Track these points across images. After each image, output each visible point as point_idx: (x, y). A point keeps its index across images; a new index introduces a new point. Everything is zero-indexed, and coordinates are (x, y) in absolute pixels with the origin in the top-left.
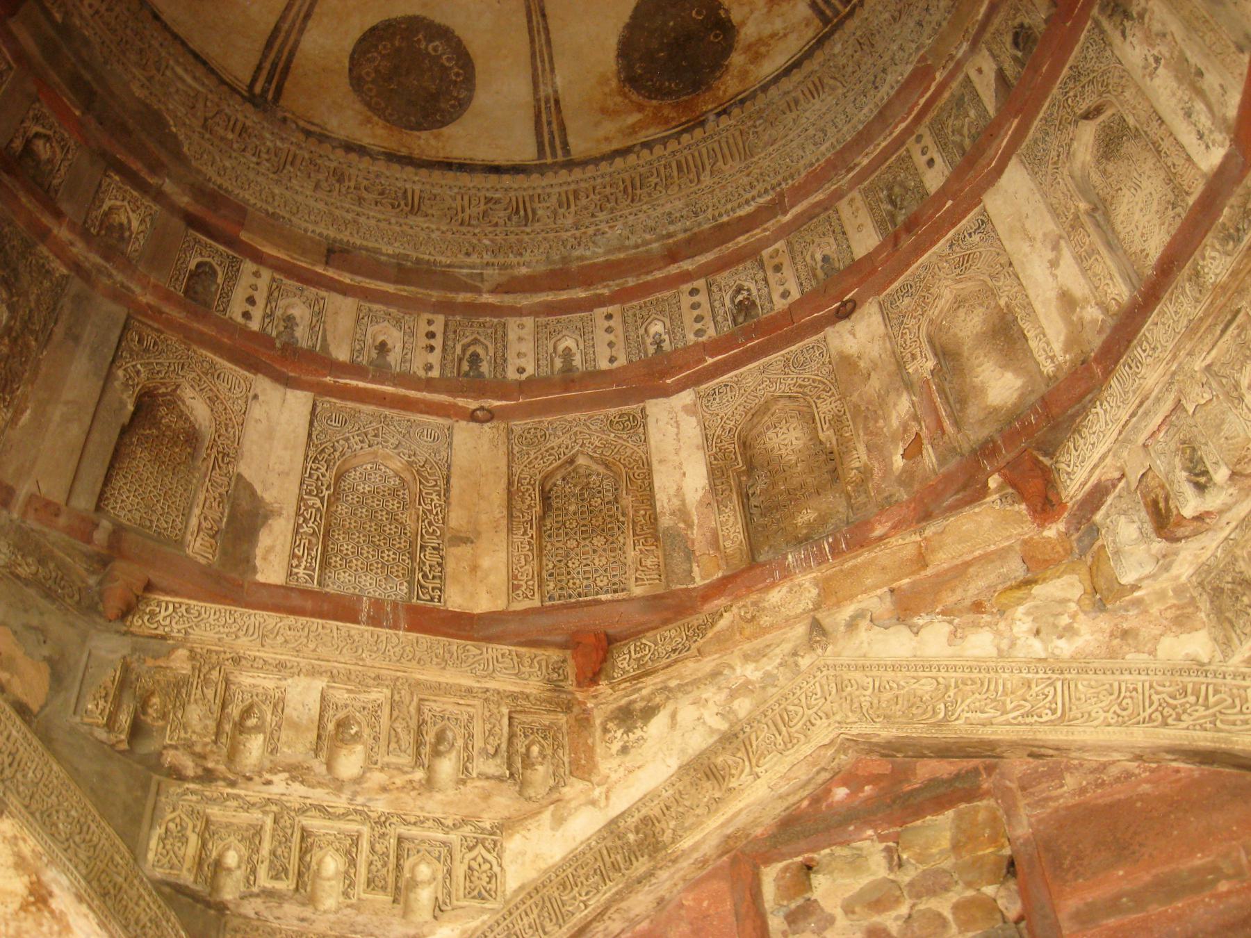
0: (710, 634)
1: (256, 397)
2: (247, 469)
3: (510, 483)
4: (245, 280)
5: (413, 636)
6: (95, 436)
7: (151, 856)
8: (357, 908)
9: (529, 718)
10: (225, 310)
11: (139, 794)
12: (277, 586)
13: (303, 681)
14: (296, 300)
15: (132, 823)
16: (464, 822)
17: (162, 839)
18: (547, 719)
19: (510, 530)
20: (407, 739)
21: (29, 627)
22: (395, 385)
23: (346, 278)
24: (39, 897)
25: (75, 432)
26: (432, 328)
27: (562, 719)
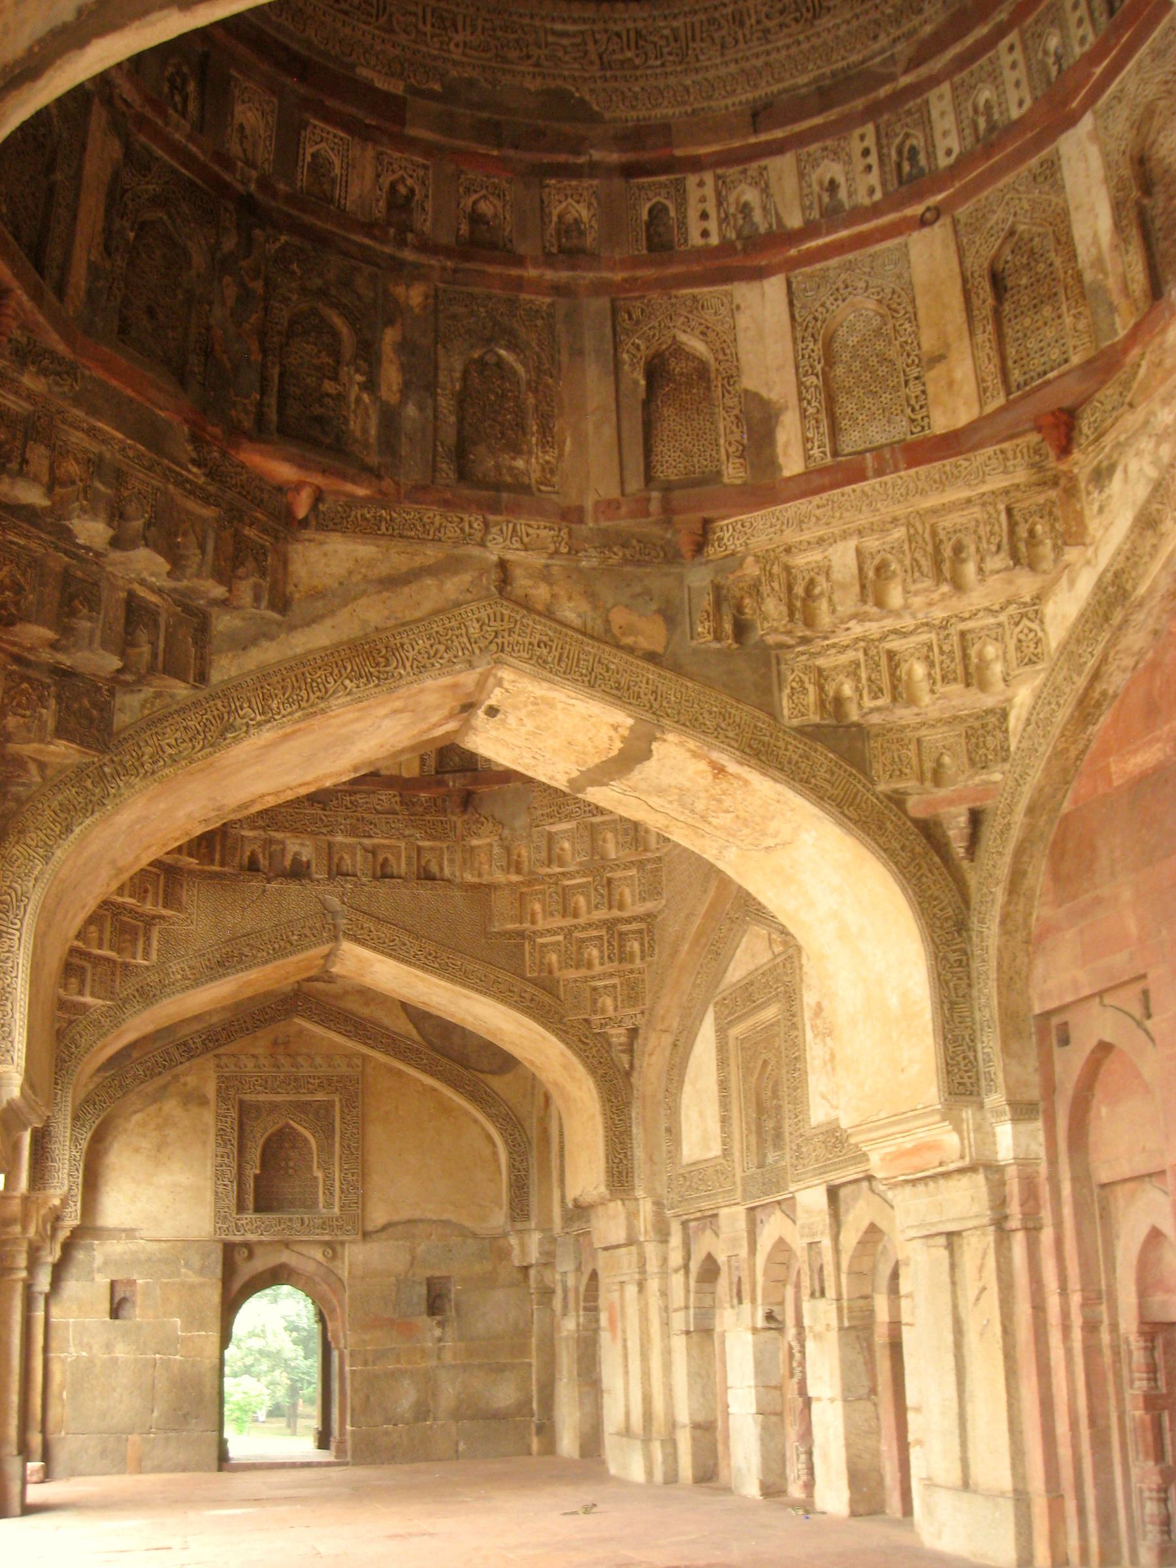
0: (1135, 385)
1: (738, 307)
2: (749, 382)
3: (965, 281)
4: (693, 194)
5: (912, 471)
6: (625, 425)
7: (786, 712)
8: (944, 696)
9: (1027, 503)
10: (686, 240)
11: (763, 670)
12: (799, 475)
13: (840, 546)
14: (743, 186)
15: (764, 696)
16: (1009, 602)
17: (790, 697)
18: (1041, 499)
19: (972, 333)
20: (926, 564)
21: (634, 596)
22: (846, 227)
23: (779, 134)
24: (719, 770)
25: (608, 432)
26: (866, 144)
27: (1053, 494)
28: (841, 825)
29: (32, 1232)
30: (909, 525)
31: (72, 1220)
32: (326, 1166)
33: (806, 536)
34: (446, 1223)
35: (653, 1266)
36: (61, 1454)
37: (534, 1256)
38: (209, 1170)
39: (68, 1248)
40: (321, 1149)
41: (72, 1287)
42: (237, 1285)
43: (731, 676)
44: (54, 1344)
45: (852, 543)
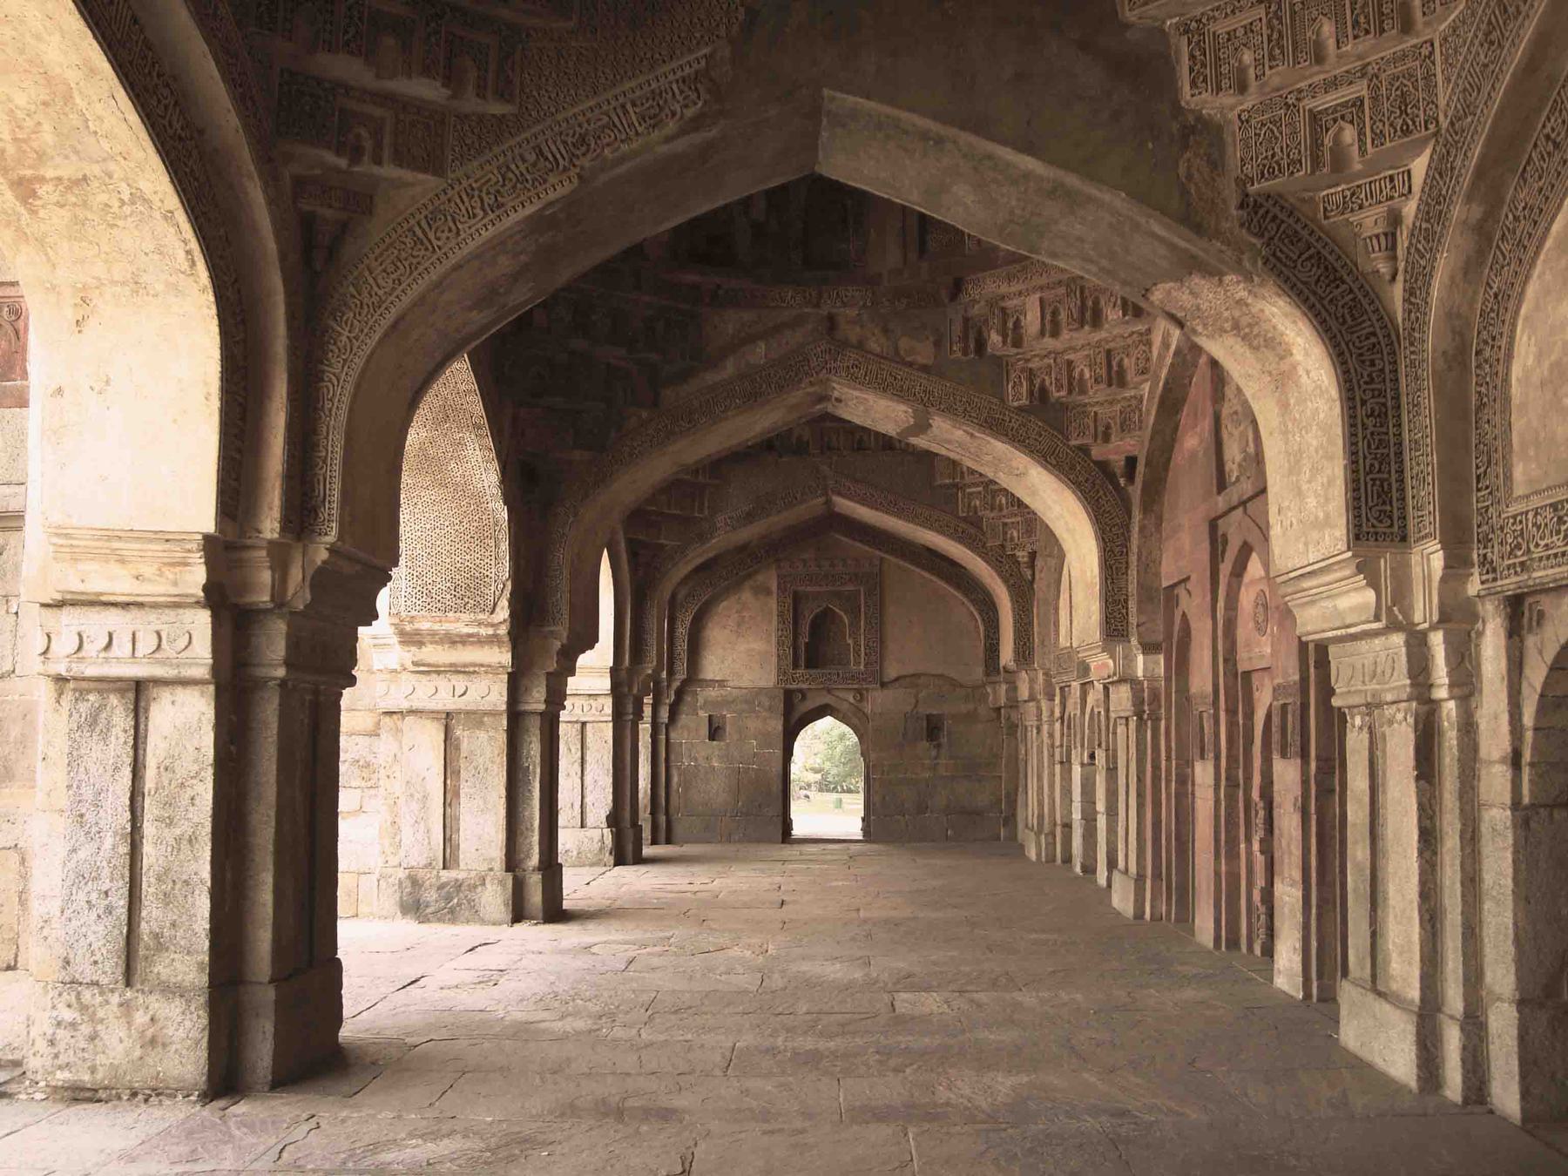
28: (1045, 468)
29: (635, 691)
30: (1068, 286)
31: (681, 675)
32: (854, 634)
33: (1013, 289)
34: (941, 676)
35: (1045, 717)
36: (679, 829)
37: (1003, 701)
38: (774, 640)
39: (680, 693)
40: (851, 624)
41: (684, 719)
42: (796, 716)
43: (978, 377)
44: (672, 757)
45: (1038, 296)
